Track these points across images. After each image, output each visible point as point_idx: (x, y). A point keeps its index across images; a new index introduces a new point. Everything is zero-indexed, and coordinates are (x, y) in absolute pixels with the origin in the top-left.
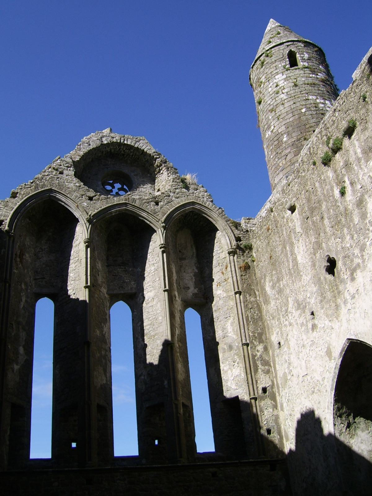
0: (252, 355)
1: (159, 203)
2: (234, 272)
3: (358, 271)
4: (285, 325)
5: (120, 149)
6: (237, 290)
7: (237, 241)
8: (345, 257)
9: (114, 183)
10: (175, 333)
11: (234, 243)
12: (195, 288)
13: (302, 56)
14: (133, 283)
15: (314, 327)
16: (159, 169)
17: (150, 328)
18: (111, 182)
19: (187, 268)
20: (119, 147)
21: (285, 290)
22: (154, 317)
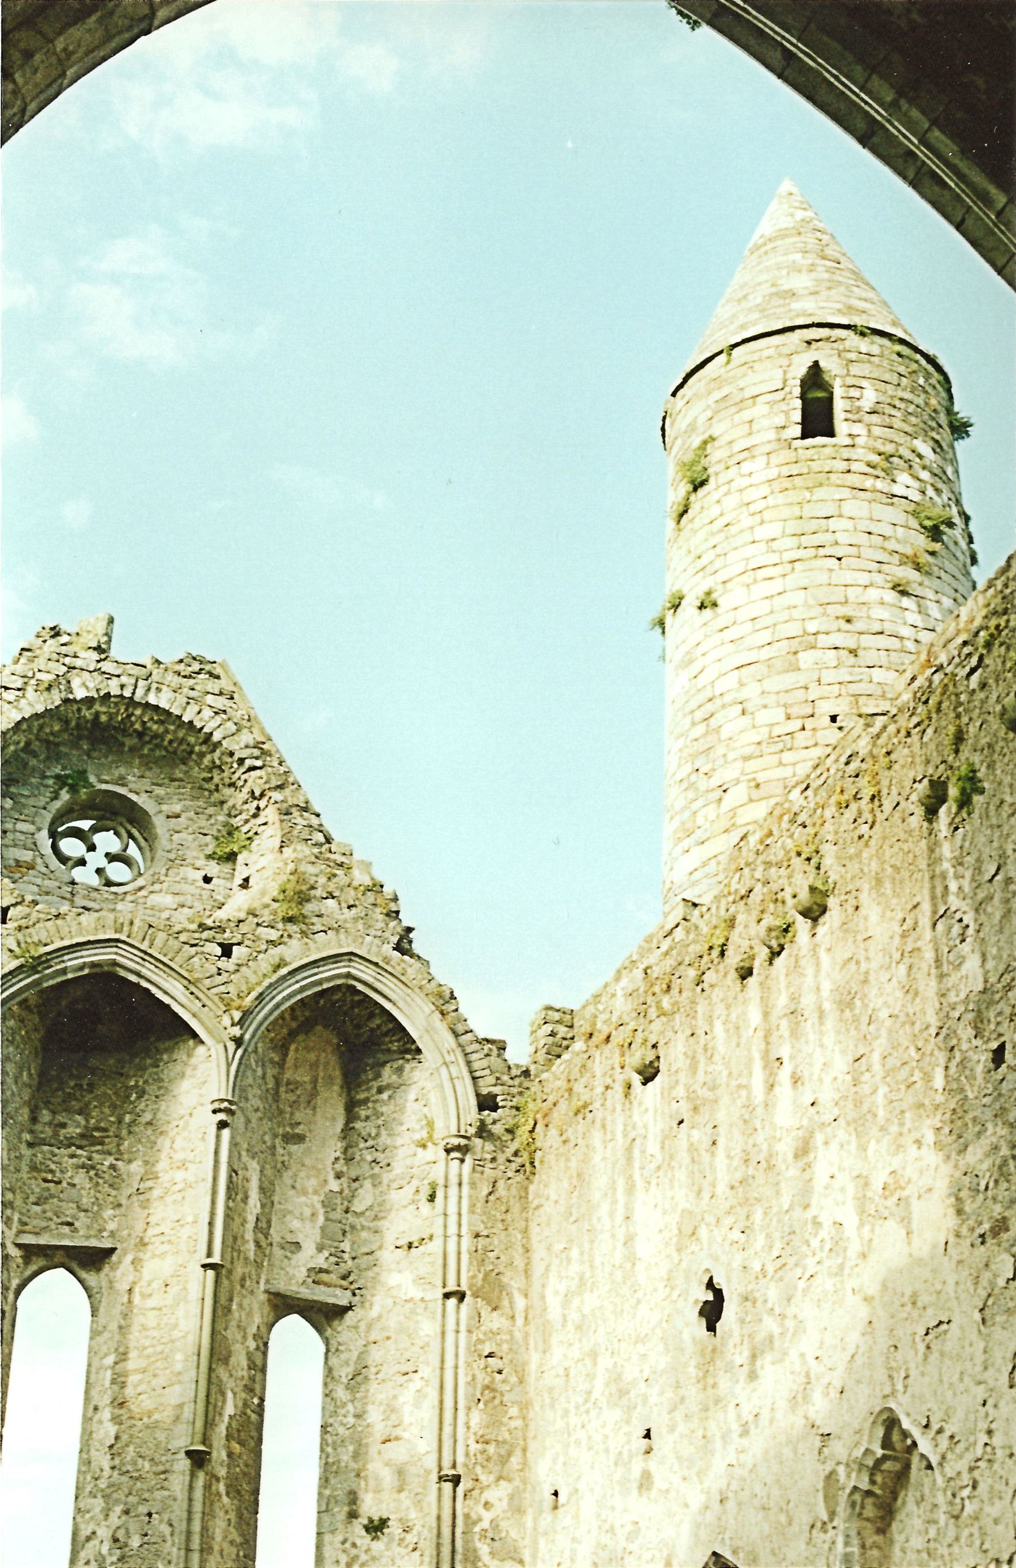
0: (467, 1516)
1: (235, 948)
2: (453, 1219)
3: (768, 1357)
4: (578, 1442)
5: (129, 716)
6: (451, 1287)
7: (481, 1108)
8: (746, 1299)
9: (95, 830)
10: (220, 1414)
11: (471, 1114)
12: (320, 1249)
13: (854, 393)
14: (111, 1212)
15: (646, 1481)
16: (258, 808)
17: (141, 1381)
18: (85, 825)
19: (302, 1174)
20: (126, 710)
21: (593, 1329)
22: (159, 1349)
